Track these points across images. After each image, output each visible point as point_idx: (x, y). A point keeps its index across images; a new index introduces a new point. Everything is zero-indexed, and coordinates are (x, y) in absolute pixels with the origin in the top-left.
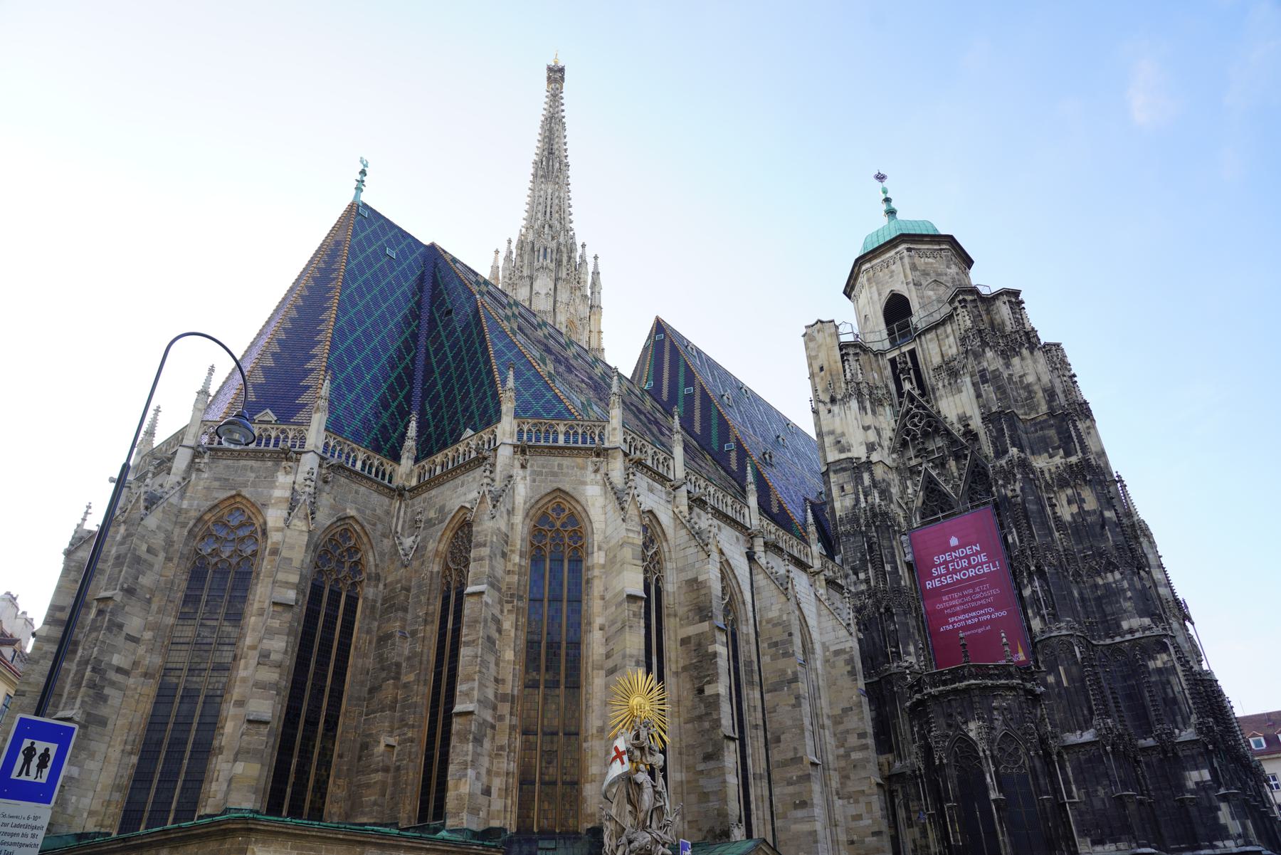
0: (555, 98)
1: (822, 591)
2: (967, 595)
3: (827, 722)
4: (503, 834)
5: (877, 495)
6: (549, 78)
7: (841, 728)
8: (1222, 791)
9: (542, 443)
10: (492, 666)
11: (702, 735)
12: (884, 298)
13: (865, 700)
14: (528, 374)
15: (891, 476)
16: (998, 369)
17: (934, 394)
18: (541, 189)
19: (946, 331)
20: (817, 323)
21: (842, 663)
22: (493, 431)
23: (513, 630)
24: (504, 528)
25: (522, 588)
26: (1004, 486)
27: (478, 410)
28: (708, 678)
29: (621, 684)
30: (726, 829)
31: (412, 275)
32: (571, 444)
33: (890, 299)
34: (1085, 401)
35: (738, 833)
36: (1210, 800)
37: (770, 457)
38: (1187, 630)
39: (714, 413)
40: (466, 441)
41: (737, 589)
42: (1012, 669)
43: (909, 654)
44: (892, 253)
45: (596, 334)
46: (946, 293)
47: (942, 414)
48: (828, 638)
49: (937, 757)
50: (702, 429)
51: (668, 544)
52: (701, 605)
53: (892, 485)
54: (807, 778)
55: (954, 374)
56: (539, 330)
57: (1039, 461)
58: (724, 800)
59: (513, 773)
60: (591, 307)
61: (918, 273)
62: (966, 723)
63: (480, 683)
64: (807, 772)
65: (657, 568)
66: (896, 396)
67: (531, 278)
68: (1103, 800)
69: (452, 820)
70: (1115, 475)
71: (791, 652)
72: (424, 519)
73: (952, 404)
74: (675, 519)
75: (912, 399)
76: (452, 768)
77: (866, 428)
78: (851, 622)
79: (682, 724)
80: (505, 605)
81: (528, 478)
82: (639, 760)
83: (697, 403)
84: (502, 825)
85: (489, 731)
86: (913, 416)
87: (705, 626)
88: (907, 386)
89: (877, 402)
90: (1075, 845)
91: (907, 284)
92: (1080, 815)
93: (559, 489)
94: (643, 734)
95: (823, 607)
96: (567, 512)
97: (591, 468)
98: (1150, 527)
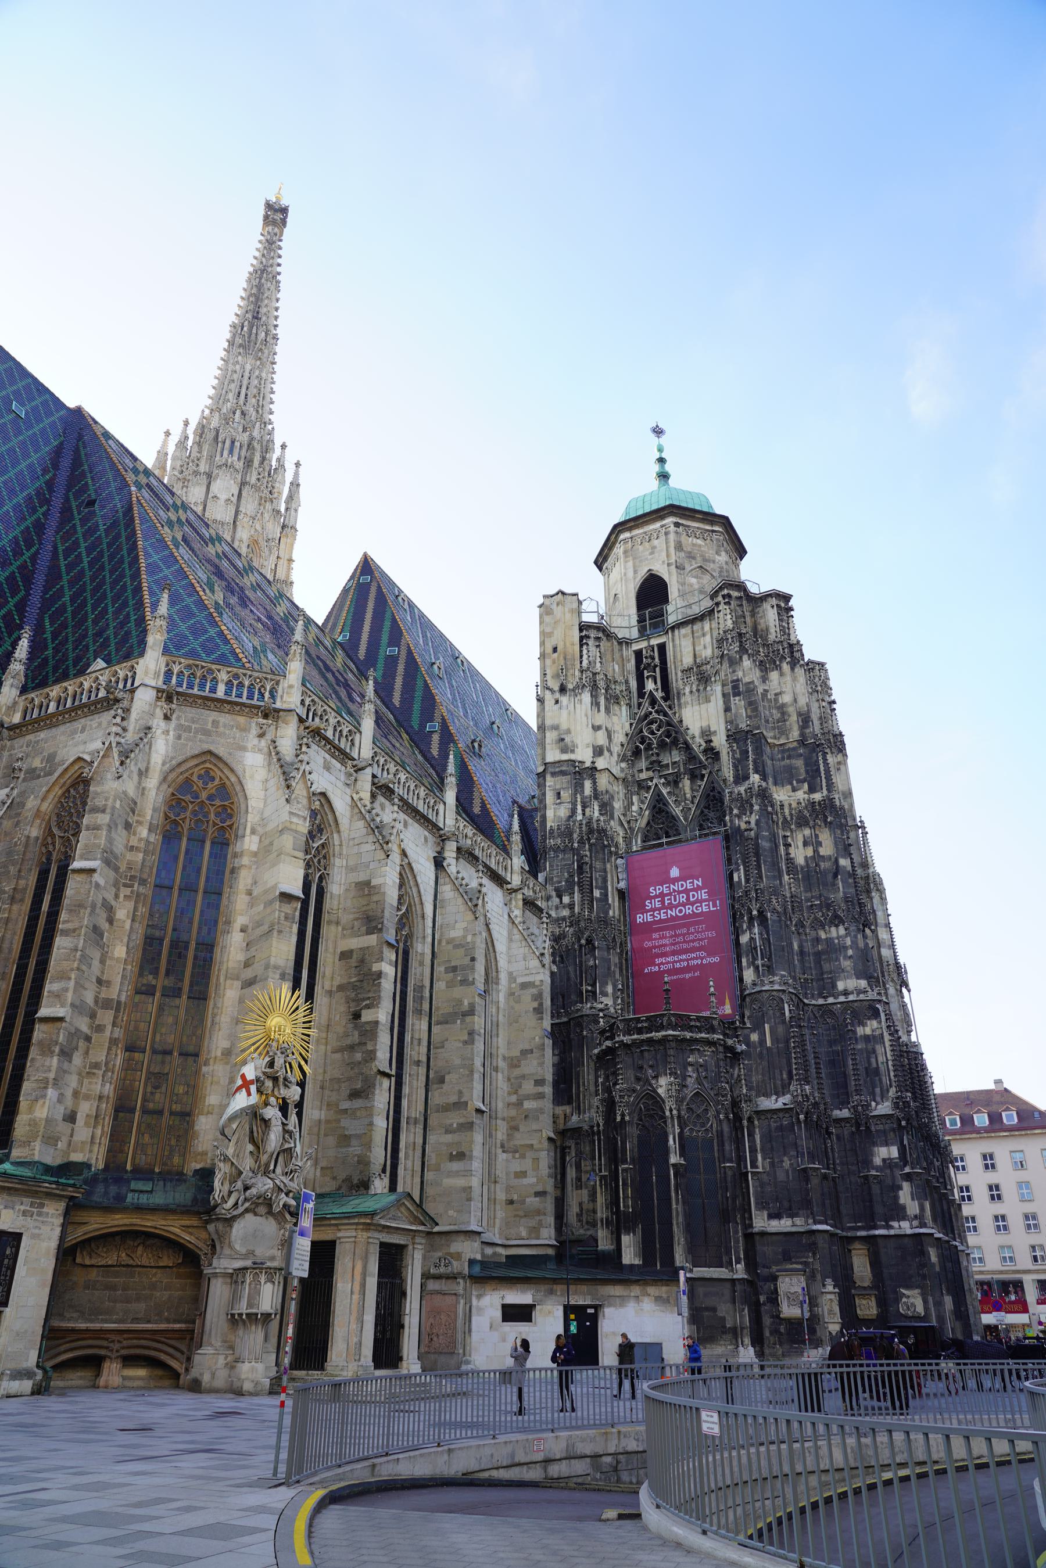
0: (271, 246)
1: (517, 912)
2: (680, 935)
3: (501, 1064)
4: (85, 1171)
5: (596, 808)
6: (266, 217)
7: (517, 1072)
8: (907, 1170)
9: (195, 691)
10: (96, 963)
11: (352, 1068)
13: (549, 1043)
14: (189, 601)
15: (615, 788)
16: (753, 682)
17: (679, 699)
18: (237, 362)
19: (703, 628)
20: (557, 594)
21: (529, 998)
22: (133, 667)
23: (129, 921)
24: (131, 792)
25: (147, 870)
26: (739, 817)
27: (115, 637)
28: (368, 1002)
29: (259, 1000)
30: (366, 1179)
31: (45, 445)
32: (233, 698)
33: (646, 580)
34: (841, 733)
35: (380, 1185)
36: (893, 1177)
37: (480, 746)
38: (903, 997)
39: (420, 683)
40: (94, 675)
41: (417, 899)
42: (716, 1023)
43: (606, 995)
44: (657, 525)
45: (286, 562)
46: (710, 584)
48: (518, 967)
49: (619, 1113)
50: (403, 700)
51: (340, 837)
52: (371, 914)
53: (616, 798)
54: (469, 1126)
55: (704, 679)
56: (210, 545)
57: (781, 793)
58: (368, 1145)
59: (108, 1097)
60: (284, 527)
61: (682, 554)
62: (656, 1077)
63: (76, 983)
64: (470, 1120)
65: (322, 864)
66: (635, 695)
67: (209, 476)
68: (787, 1172)
69: (19, 1150)
70: (858, 819)
72: (25, 767)
73: (696, 714)
74: (352, 807)
75: (653, 702)
76: (26, 1086)
77: (596, 728)
78: (546, 951)
79: (329, 1053)
80: (122, 888)
81: (171, 733)
82: (270, 1092)
83: (401, 668)
84: (85, 1160)
85: (82, 1044)
86: (651, 722)
87: (372, 940)
88: (650, 686)
89: (613, 699)
90: (751, 1218)
91: (669, 565)
92: (762, 1187)
93: (210, 752)
94: (279, 1061)
95: (515, 931)
96: (217, 781)
97: (254, 731)
98: (884, 882)
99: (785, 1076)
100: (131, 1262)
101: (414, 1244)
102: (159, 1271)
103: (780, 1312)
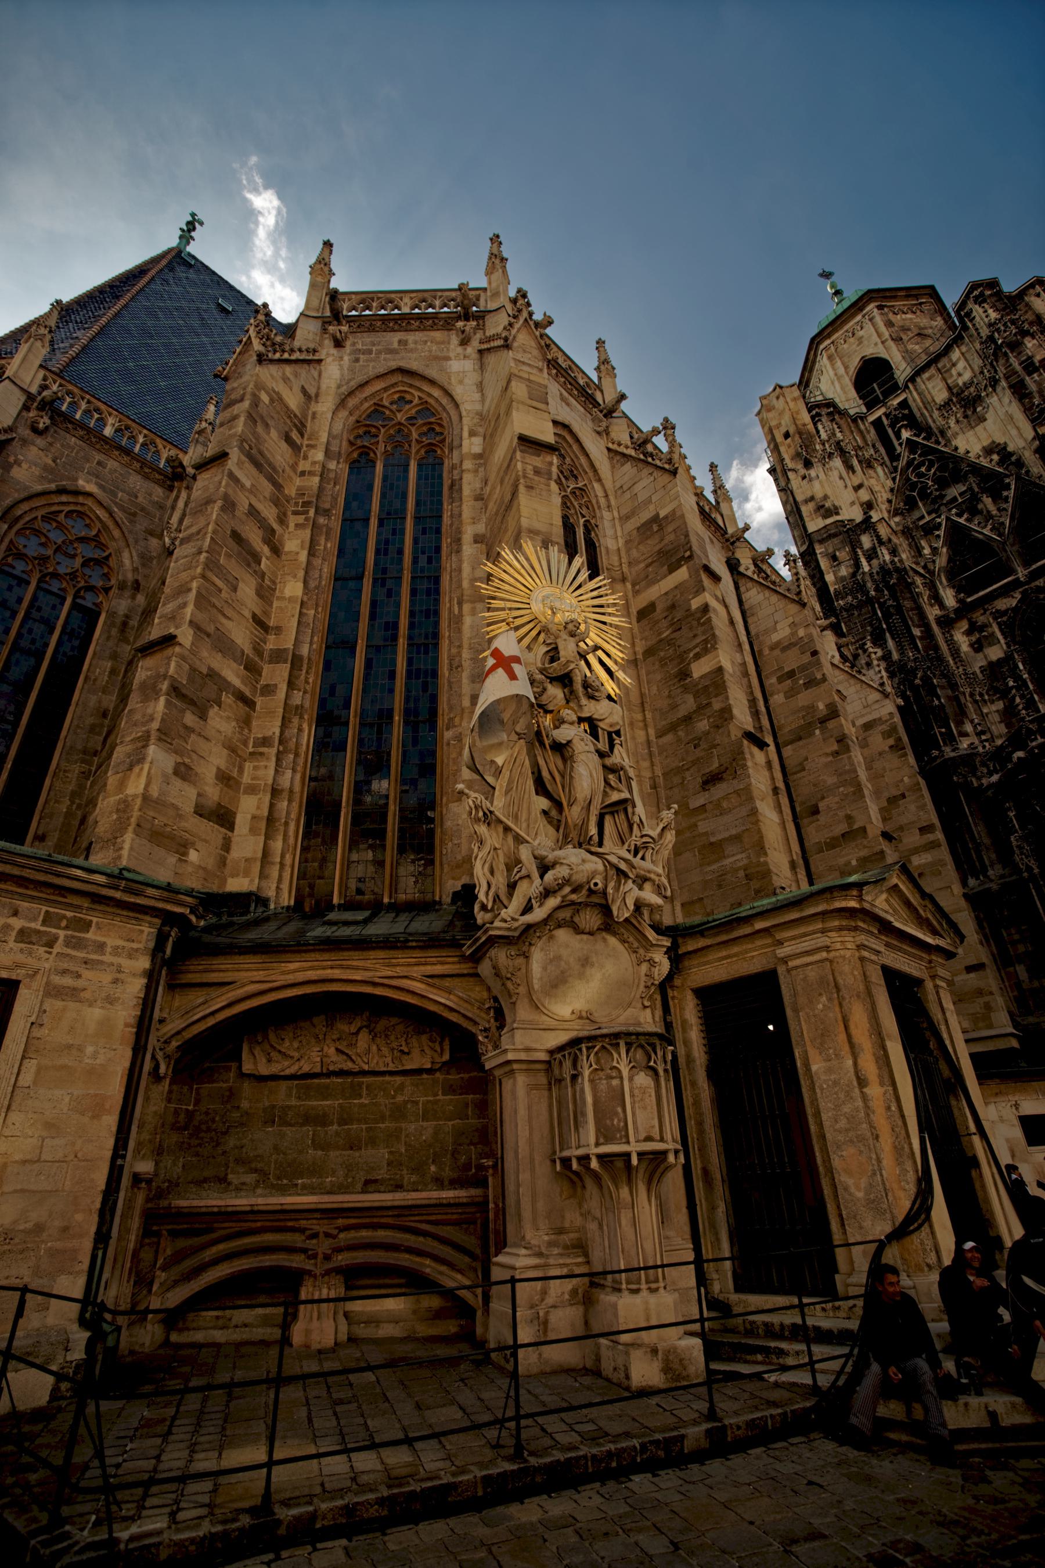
5: (885, 552)
10: (247, 590)
21: (879, 738)
43: (966, 735)
44: (859, 318)
47: (961, 451)
51: (603, 486)
58: (761, 847)
59: (291, 791)
64: (877, 849)
71: (819, 676)
74: (611, 459)
79: (652, 738)
81: (346, 358)
85: (227, 699)
86: (919, 466)
87: (682, 574)
97: (455, 340)
100: (349, 1065)
101: (933, 977)
102: (408, 1080)
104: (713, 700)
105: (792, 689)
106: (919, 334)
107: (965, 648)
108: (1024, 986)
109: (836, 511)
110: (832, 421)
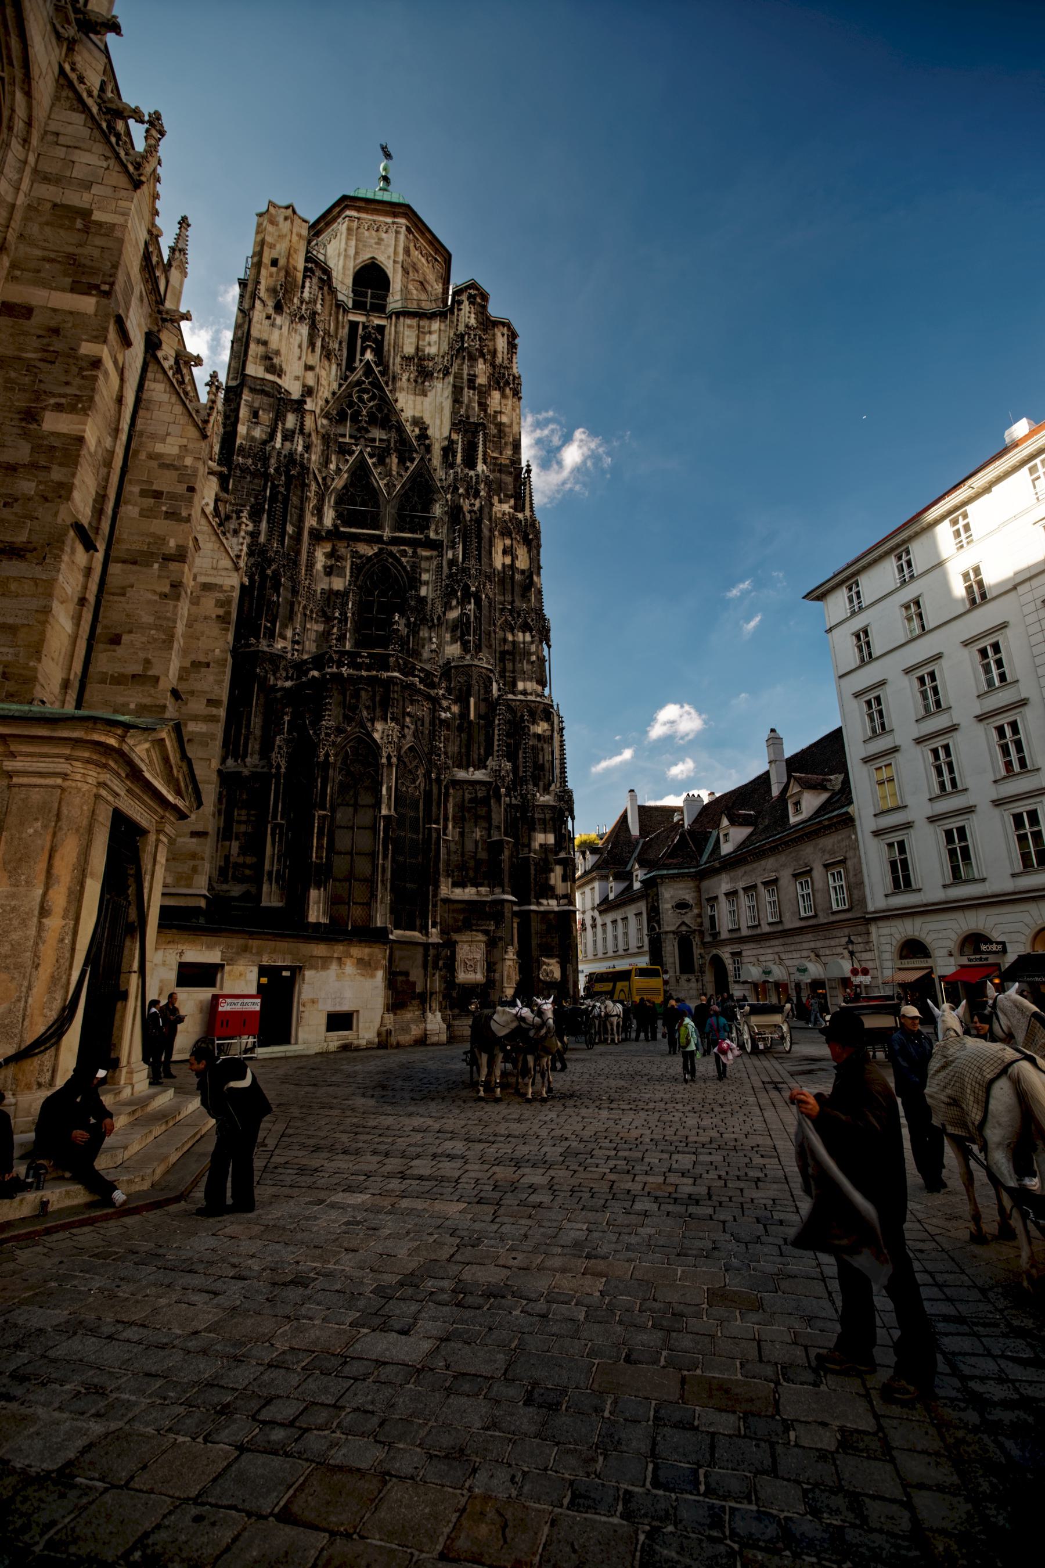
5: (301, 442)
12: (361, 260)
19: (430, 327)
20: (287, 208)
21: (212, 603)
28: (63, 401)
43: (284, 638)
44: (389, 220)
47: (399, 405)
58: (37, 650)
62: (372, 721)
64: (161, 702)
68: (476, 842)
71: (184, 514)
87: (88, 304)
89: (328, 354)
91: (395, 262)
99: (482, 751)
103: (454, 977)
104: (55, 467)
105: (151, 510)
106: (421, 283)
107: (319, 566)
108: (232, 859)
109: (280, 372)
110: (321, 288)
